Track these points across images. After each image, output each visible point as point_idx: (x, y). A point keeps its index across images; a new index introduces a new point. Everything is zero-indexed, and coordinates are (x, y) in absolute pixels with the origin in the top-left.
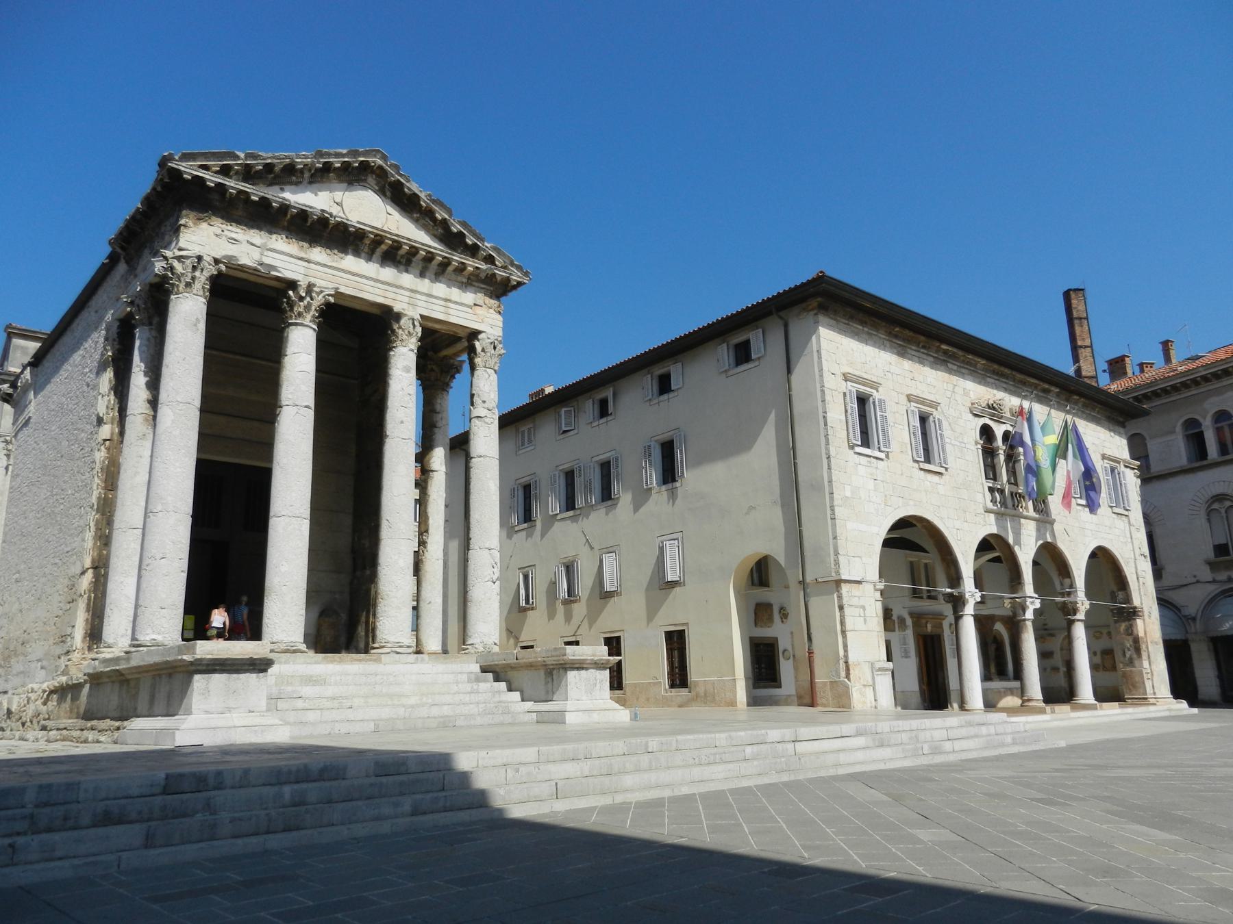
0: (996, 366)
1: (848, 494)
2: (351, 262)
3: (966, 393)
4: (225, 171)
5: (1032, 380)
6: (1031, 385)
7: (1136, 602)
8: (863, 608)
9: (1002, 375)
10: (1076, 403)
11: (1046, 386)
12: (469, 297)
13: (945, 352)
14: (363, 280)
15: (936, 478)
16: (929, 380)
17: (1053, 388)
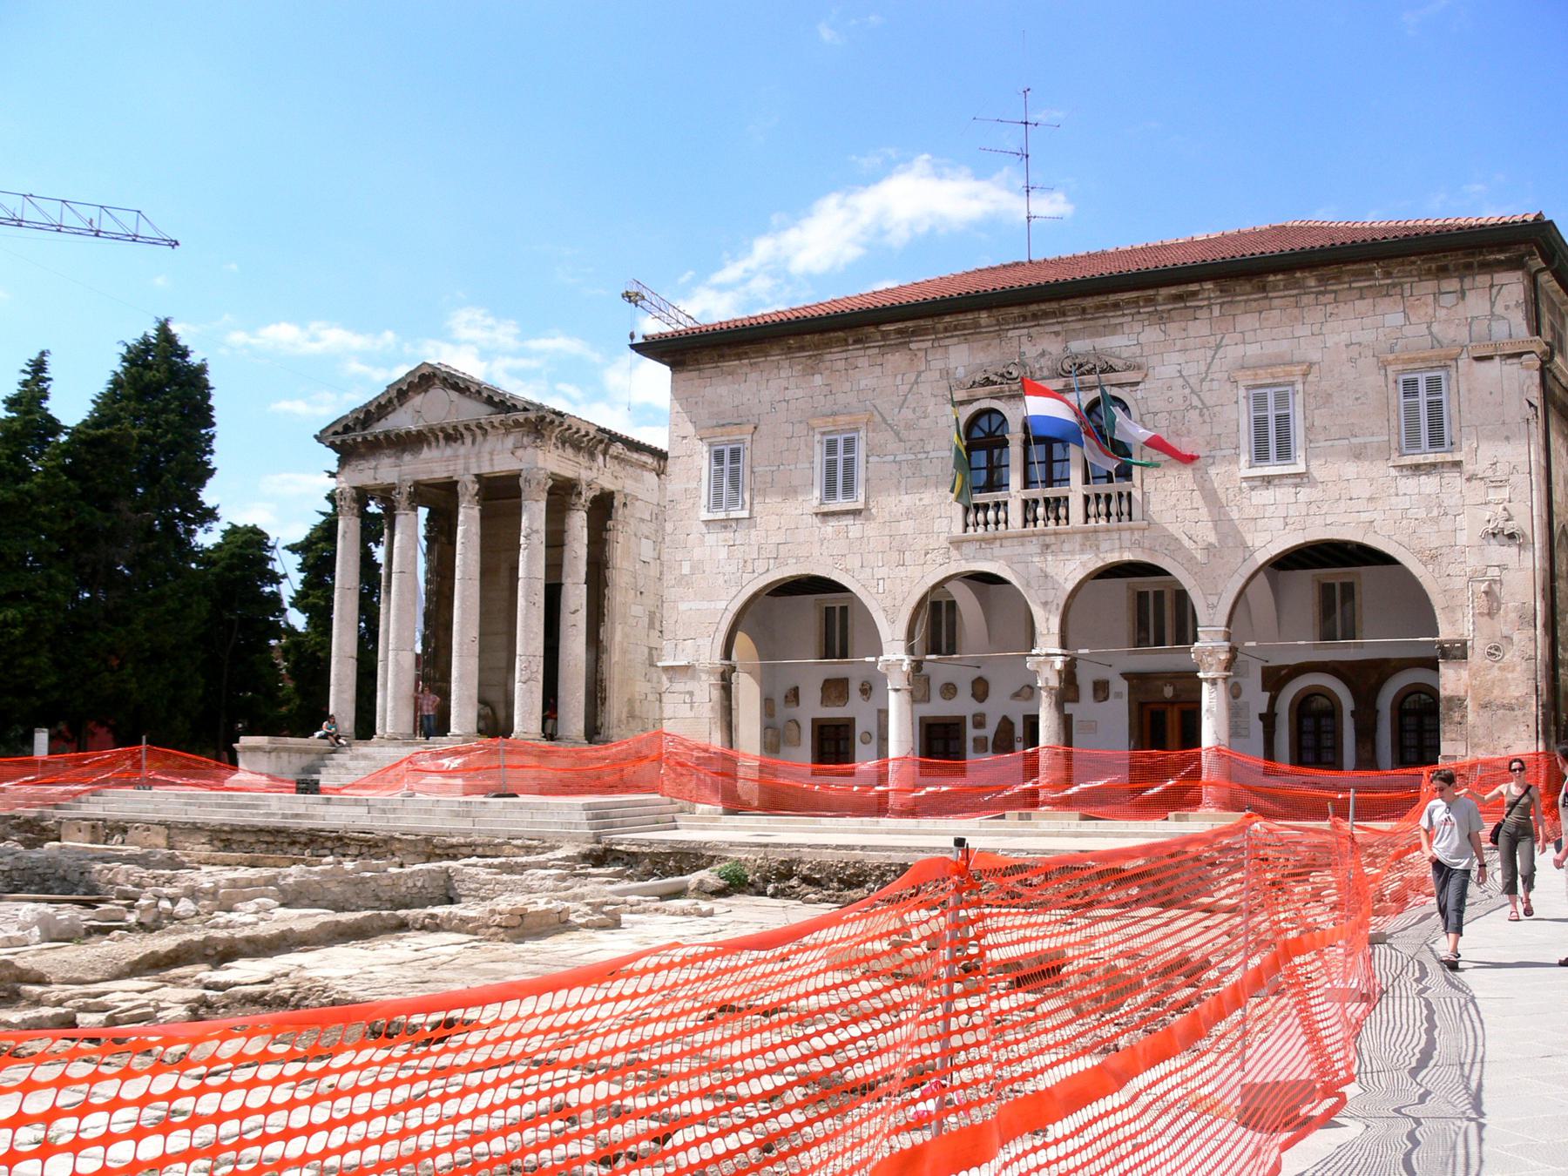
0: (1016, 311)
1: (686, 570)
2: (426, 453)
3: (946, 373)
4: (347, 429)
5: (1126, 296)
6: (1135, 302)
7: (1446, 632)
8: (691, 694)
9: (1046, 315)
10: (1275, 289)
11: (1173, 290)
12: (510, 442)
13: (899, 332)
14: (432, 464)
15: (849, 520)
16: (863, 384)
17: (1194, 287)
